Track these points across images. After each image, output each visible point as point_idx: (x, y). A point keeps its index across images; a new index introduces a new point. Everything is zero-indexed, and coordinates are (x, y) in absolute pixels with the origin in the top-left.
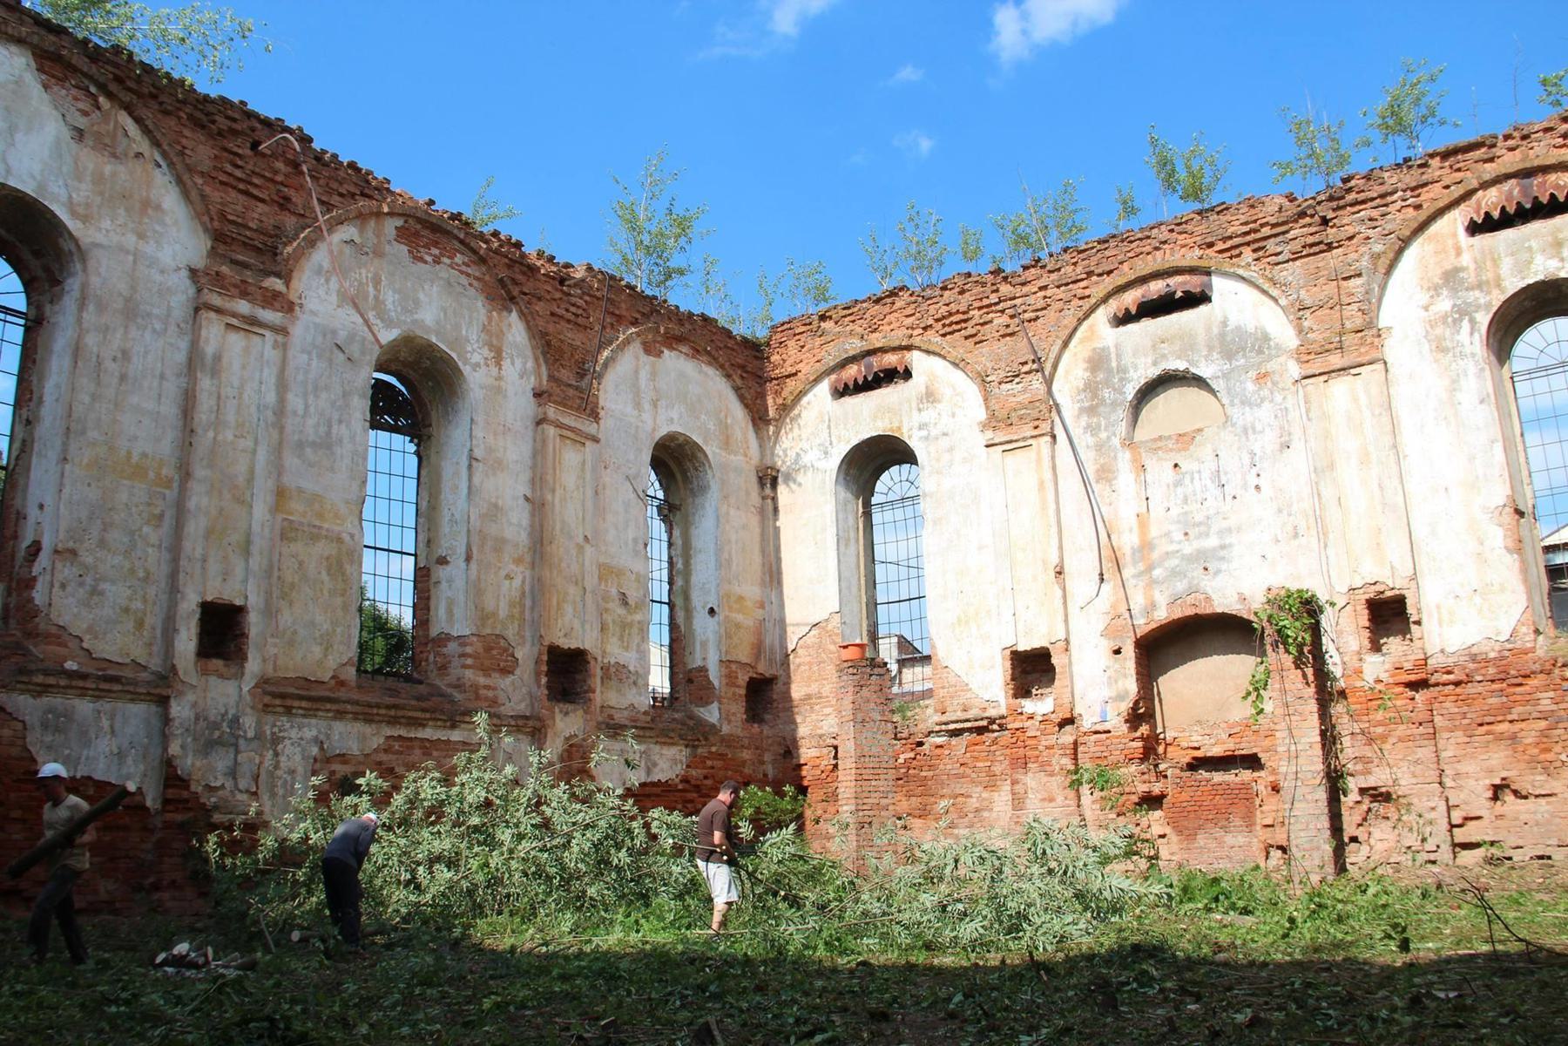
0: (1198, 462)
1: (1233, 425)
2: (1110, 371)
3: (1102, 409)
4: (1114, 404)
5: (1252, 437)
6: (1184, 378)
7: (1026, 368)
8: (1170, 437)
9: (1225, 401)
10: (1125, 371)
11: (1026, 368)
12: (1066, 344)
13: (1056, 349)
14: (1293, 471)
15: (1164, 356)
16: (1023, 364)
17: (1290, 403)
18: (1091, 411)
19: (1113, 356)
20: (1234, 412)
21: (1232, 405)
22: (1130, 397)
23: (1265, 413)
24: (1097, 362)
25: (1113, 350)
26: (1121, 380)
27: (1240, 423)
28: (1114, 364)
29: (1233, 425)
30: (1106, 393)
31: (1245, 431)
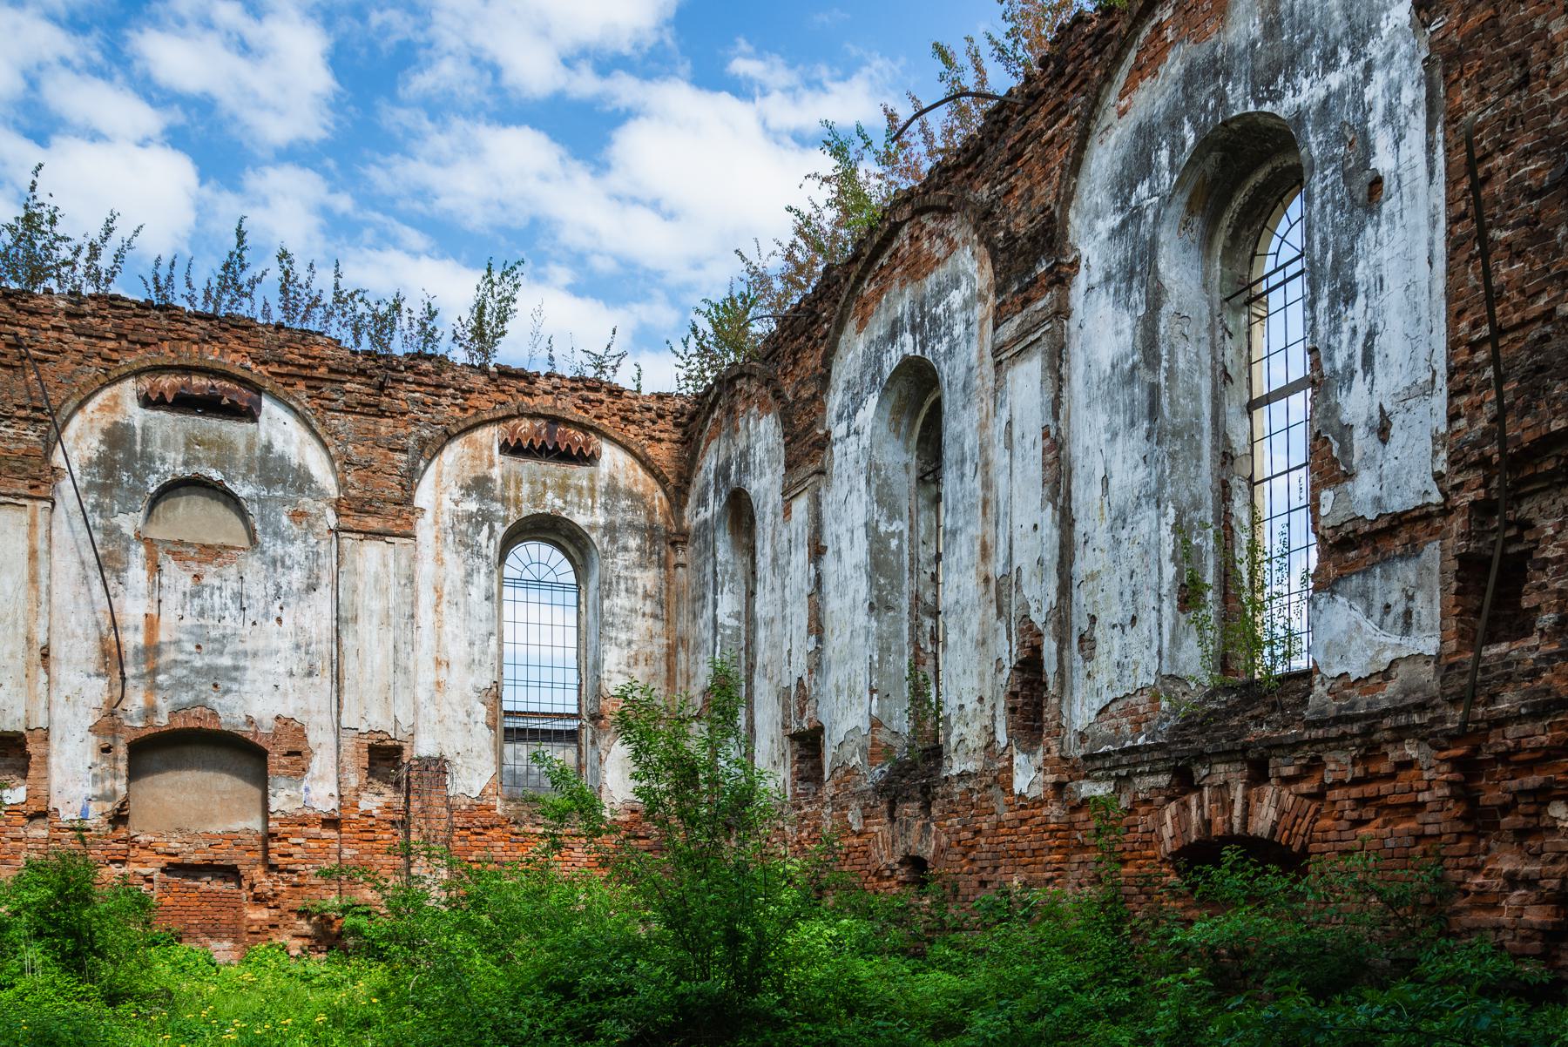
0: (221, 580)
1: (263, 553)
2: (131, 454)
3: (116, 491)
4: (134, 491)
5: (280, 570)
6: (213, 488)
7: (22, 413)
8: (191, 545)
9: (258, 526)
10: (151, 459)
11: (22, 413)
12: (80, 406)
13: (71, 405)
14: (316, 616)
15: (198, 459)
16: (23, 407)
17: (322, 548)
18: (103, 489)
19: (138, 439)
20: (266, 541)
21: (264, 532)
22: (152, 490)
23: (297, 550)
24: (117, 437)
25: (139, 431)
26: (144, 467)
27: (271, 552)
28: (138, 448)
29: (263, 553)
30: (125, 476)
31: (274, 562)
